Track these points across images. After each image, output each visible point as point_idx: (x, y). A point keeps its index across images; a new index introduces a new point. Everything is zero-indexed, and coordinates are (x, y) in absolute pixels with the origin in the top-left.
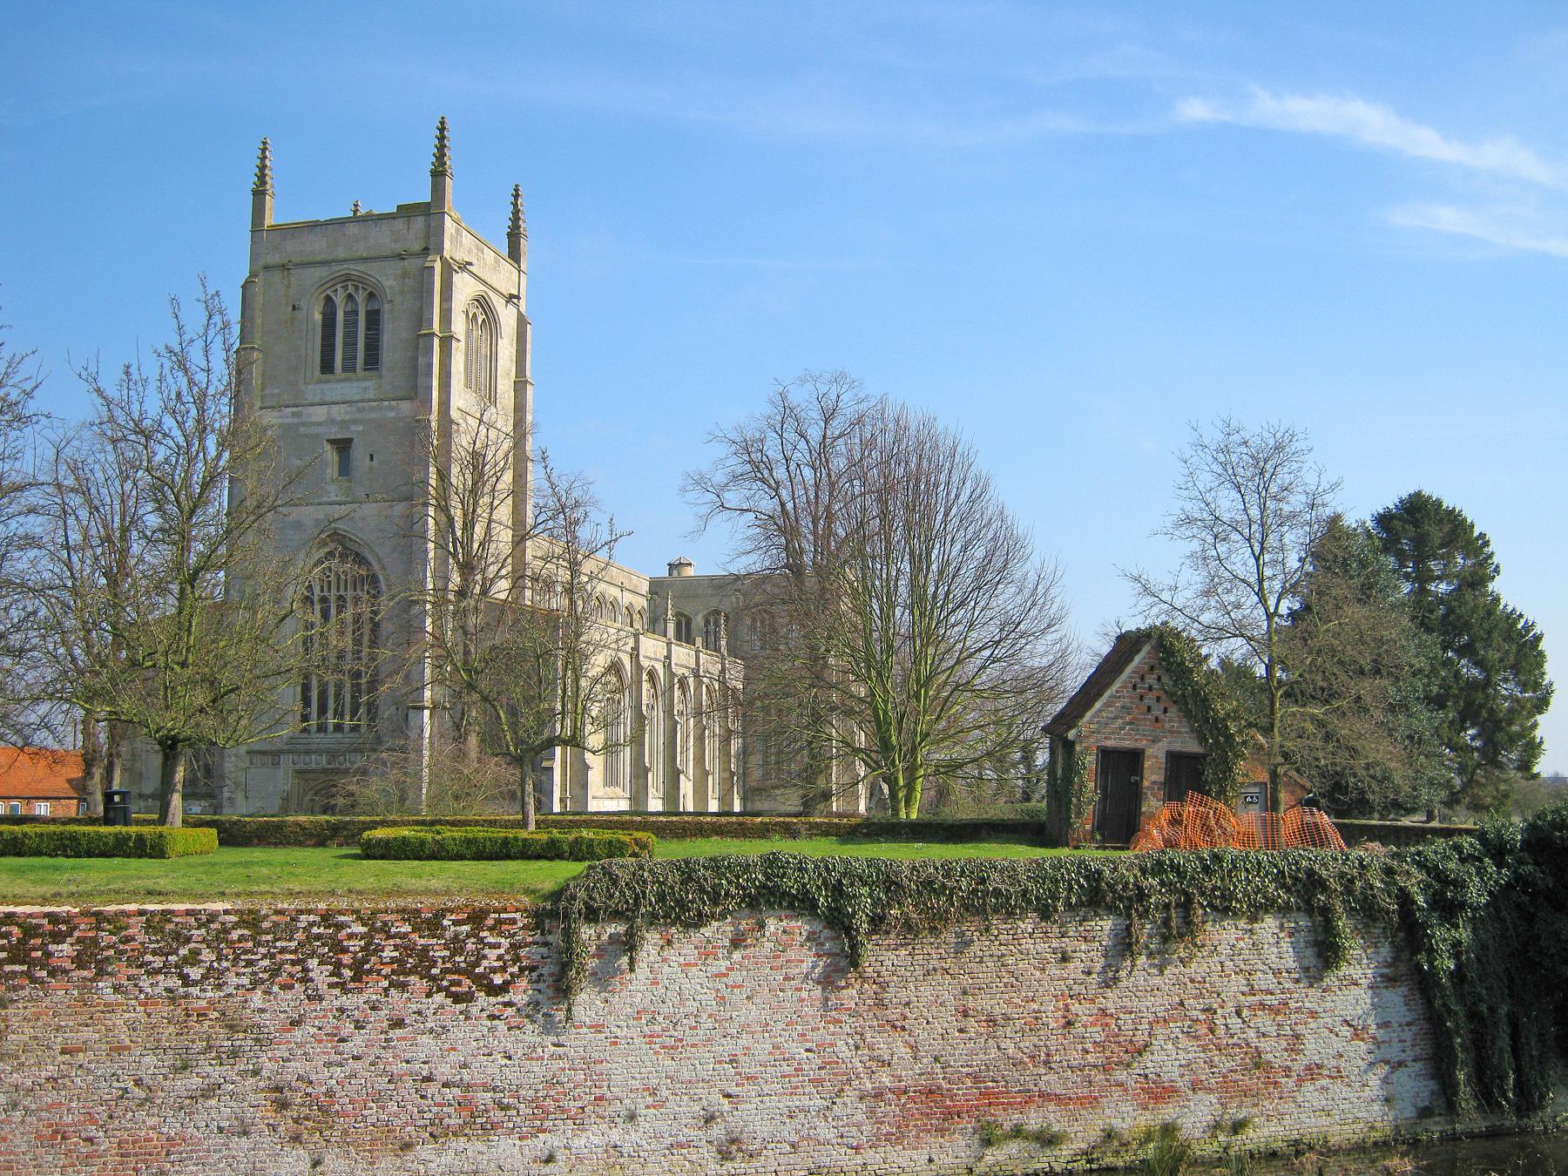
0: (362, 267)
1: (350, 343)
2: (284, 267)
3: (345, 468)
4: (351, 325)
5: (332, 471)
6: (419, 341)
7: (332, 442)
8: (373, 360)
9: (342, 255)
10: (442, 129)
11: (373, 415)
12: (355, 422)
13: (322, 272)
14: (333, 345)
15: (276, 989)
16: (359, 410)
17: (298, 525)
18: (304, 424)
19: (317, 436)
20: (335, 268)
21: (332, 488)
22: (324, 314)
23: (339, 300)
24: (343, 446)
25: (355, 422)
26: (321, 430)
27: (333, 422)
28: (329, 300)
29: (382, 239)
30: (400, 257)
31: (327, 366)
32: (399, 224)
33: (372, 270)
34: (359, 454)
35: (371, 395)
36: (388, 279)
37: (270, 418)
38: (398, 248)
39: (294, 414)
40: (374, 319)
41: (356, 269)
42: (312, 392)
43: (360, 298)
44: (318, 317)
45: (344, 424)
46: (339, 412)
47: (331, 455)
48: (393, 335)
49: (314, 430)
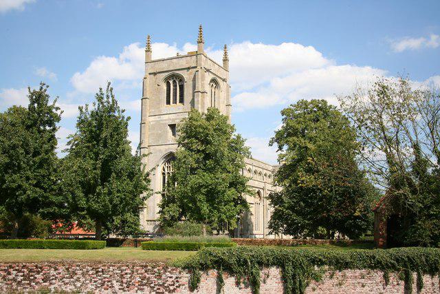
0: (177, 72)
2: (155, 74)
4: (175, 90)
8: (182, 101)
13: (167, 74)
15: (103, 290)
23: (171, 82)
24: (173, 127)
26: (167, 122)
29: (183, 63)
30: (189, 68)
31: (168, 103)
33: (180, 72)
36: (185, 74)
37: (152, 119)
40: (182, 88)
44: (165, 88)
45: (173, 120)
47: (170, 131)
49: (165, 122)
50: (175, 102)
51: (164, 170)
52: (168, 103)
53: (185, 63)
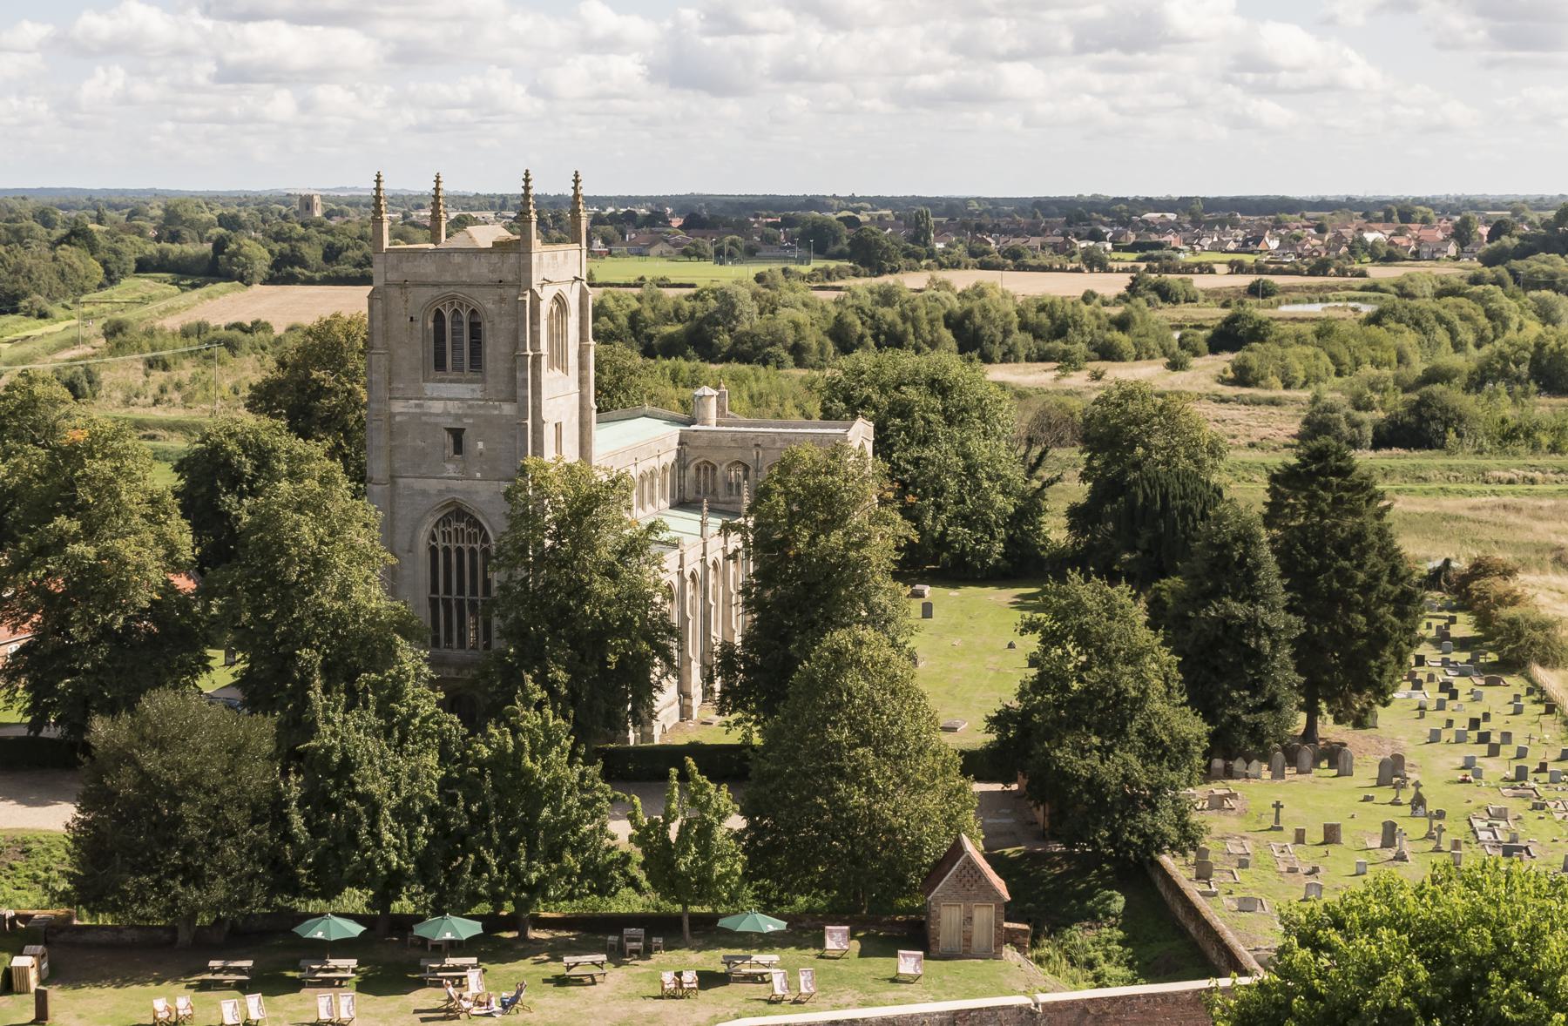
0: (466, 290)
1: (457, 347)
2: (403, 285)
3: (458, 447)
5: (450, 451)
6: (516, 359)
7: (450, 430)
8: (477, 362)
9: (448, 278)
10: (527, 181)
11: (482, 412)
12: (466, 416)
13: (434, 292)
14: (444, 348)
16: (470, 407)
17: (424, 493)
18: (425, 414)
19: (437, 425)
20: (444, 290)
21: (450, 467)
22: (435, 321)
23: (447, 314)
24: (457, 435)
25: (466, 416)
26: (439, 420)
27: (449, 414)
28: (438, 311)
31: (440, 364)
32: (495, 258)
34: (467, 438)
35: (478, 395)
36: (487, 303)
38: (495, 277)
39: (417, 406)
41: (462, 292)
42: (430, 388)
43: (465, 315)
44: (431, 325)
45: (458, 417)
46: (453, 407)
48: (494, 348)
49: (432, 420)
50: (458, 368)
51: (434, 538)
52: (440, 364)
53: (485, 270)
